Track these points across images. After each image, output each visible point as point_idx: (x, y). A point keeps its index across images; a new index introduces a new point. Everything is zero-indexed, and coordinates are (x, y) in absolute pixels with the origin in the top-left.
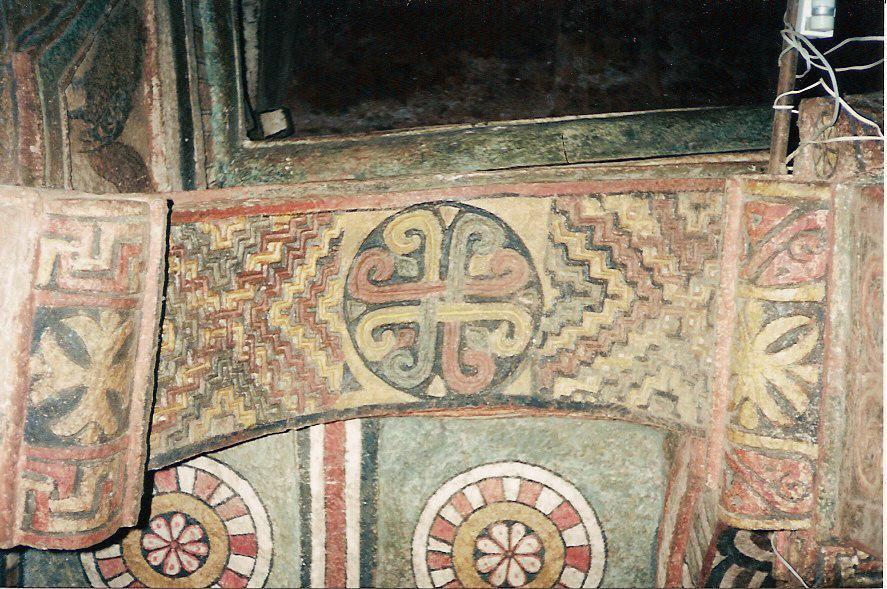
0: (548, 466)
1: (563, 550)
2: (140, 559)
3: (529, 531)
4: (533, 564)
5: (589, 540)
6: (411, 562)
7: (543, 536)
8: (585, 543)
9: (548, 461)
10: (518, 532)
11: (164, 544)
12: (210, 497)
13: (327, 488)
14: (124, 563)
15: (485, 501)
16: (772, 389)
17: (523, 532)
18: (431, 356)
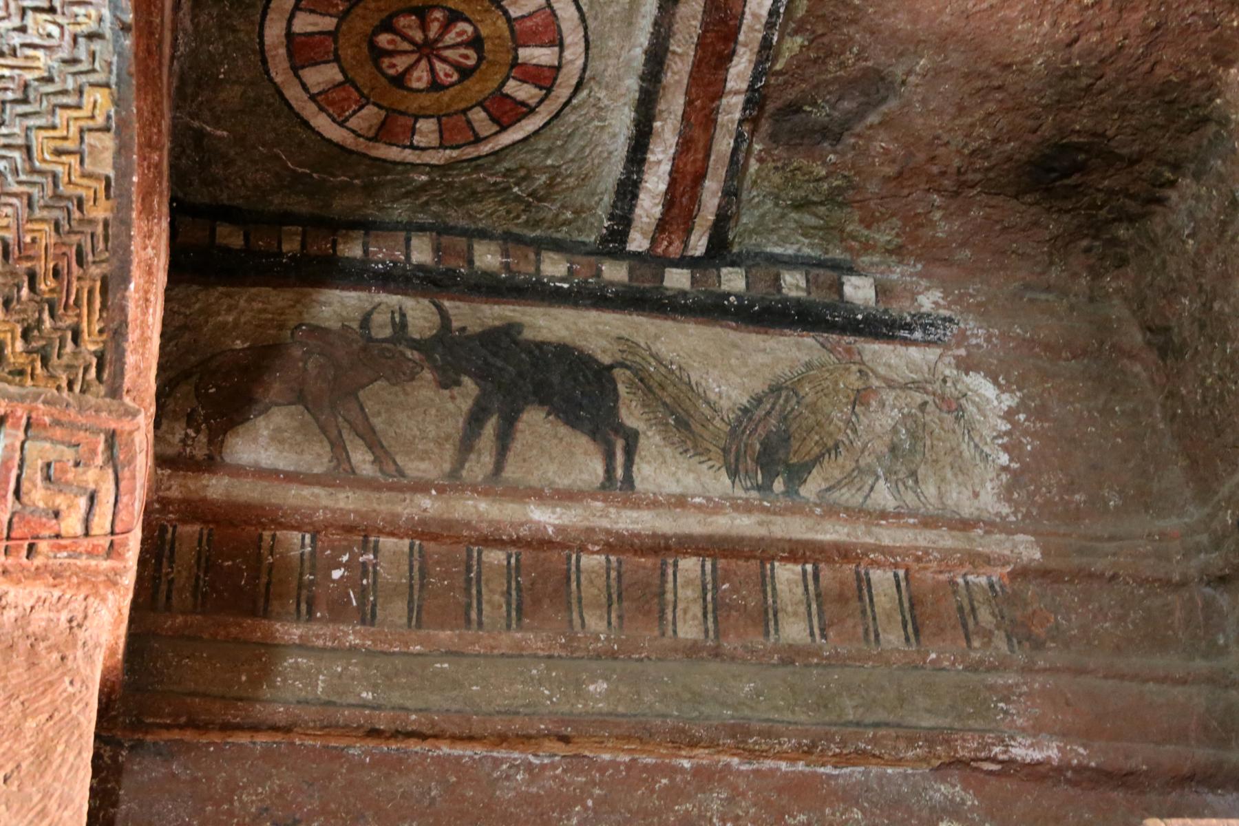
2: (446, 96)
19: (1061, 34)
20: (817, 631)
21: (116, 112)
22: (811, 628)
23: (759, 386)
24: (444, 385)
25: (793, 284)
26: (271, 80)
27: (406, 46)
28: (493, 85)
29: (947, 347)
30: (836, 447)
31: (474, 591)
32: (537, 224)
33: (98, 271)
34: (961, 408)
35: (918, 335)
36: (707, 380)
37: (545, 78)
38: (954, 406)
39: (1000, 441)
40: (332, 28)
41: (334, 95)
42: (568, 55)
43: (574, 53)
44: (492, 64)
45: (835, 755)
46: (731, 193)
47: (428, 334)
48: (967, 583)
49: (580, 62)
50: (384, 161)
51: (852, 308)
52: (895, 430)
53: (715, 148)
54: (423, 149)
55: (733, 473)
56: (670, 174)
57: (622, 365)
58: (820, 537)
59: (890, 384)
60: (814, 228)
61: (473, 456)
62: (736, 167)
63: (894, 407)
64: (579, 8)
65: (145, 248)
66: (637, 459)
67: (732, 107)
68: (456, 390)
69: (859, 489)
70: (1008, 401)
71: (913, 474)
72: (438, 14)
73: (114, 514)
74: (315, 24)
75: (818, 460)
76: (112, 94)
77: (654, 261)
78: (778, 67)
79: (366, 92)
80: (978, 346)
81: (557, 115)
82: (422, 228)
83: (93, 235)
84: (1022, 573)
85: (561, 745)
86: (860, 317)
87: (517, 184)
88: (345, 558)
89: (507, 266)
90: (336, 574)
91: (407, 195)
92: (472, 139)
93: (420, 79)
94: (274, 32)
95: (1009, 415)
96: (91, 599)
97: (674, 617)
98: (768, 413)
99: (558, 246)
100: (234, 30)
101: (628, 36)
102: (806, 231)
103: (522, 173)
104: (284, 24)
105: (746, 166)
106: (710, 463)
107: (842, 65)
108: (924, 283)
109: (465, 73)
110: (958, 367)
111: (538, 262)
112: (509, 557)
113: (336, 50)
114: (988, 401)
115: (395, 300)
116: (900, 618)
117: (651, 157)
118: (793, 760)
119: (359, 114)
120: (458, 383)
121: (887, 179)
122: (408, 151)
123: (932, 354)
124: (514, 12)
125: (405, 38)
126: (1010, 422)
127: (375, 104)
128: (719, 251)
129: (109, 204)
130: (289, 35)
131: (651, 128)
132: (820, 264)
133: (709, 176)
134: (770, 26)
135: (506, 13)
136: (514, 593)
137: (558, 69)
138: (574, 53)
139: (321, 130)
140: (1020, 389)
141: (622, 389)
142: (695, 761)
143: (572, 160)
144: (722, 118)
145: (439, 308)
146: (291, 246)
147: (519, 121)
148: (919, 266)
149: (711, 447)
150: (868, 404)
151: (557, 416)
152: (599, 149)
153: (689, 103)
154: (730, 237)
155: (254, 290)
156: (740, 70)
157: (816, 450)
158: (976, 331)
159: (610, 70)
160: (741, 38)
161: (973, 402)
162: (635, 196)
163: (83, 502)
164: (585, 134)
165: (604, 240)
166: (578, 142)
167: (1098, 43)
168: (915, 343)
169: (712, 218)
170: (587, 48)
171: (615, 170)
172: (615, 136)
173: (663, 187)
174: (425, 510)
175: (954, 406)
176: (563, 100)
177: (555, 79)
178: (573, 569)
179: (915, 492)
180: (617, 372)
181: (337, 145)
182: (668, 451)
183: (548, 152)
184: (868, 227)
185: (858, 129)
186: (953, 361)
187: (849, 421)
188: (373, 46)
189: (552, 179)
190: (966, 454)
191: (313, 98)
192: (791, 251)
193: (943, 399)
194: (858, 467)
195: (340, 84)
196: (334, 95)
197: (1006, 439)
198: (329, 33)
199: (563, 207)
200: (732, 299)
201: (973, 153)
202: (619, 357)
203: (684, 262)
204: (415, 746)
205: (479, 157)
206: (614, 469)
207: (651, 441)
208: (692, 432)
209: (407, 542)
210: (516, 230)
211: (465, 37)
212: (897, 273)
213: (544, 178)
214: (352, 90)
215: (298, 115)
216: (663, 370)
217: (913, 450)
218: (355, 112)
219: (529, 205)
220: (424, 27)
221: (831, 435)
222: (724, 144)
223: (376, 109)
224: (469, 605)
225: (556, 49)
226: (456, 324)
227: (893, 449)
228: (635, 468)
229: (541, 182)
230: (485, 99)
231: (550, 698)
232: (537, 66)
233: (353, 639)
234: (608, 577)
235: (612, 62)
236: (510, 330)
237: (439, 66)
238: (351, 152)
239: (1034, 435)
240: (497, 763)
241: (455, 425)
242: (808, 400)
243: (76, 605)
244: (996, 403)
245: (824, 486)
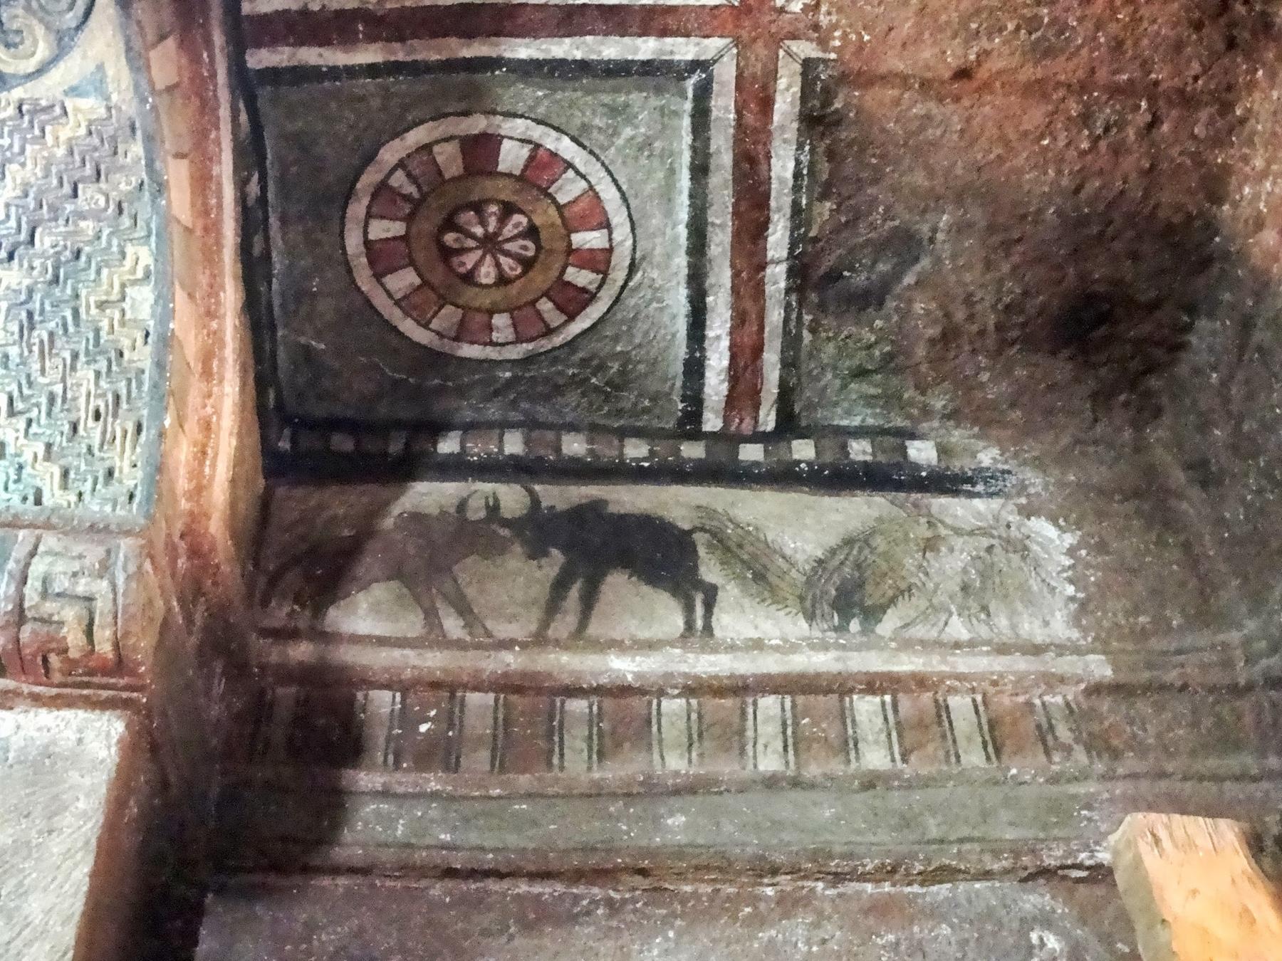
2: (514, 289)
12: (407, 198)
14: (519, 308)
19: (1065, 182)
20: (898, 757)
22: (892, 754)
23: (833, 540)
24: (532, 557)
25: (860, 450)
26: (358, 289)
28: (554, 273)
29: (1008, 497)
30: (909, 590)
31: (556, 739)
32: (619, 413)
34: (1026, 548)
35: (980, 488)
36: (782, 538)
37: (599, 261)
38: (1019, 547)
39: (1065, 575)
40: (402, 232)
41: (416, 299)
42: (617, 236)
43: (622, 233)
44: (551, 252)
45: (920, 873)
46: (789, 363)
47: (518, 514)
48: (1043, 704)
49: (629, 242)
51: (917, 467)
52: (965, 571)
53: (767, 321)
54: (503, 345)
55: (810, 617)
56: (731, 348)
57: (702, 529)
58: (895, 668)
59: (958, 532)
60: (873, 397)
61: (558, 616)
62: (791, 341)
63: (962, 551)
64: (619, 189)
65: (205, 406)
66: (716, 610)
67: (777, 277)
68: (544, 561)
69: (933, 625)
70: (1069, 539)
71: (985, 609)
72: (494, 208)
74: (388, 230)
75: (893, 601)
77: (729, 439)
78: (812, 234)
80: (1038, 495)
81: (617, 300)
82: (513, 426)
84: (1096, 690)
85: (638, 878)
86: (924, 474)
87: (595, 375)
88: (433, 713)
89: (591, 452)
90: (424, 728)
91: (496, 393)
93: (487, 274)
94: (353, 242)
95: (1071, 552)
97: (755, 752)
98: (842, 563)
99: (639, 433)
101: (669, 213)
102: (869, 400)
103: (595, 362)
105: (799, 337)
106: (788, 610)
107: (873, 227)
108: (981, 444)
109: (528, 264)
110: (1020, 513)
111: (623, 446)
112: (590, 707)
114: (1052, 541)
115: (487, 487)
116: (980, 739)
117: (710, 333)
118: (878, 881)
120: (546, 554)
121: (932, 342)
122: (489, 349)
123: (996, 503)
124: (562, 199)
126: (1072, 557)
127: (452, 304)
128: (789, 425)
130: (367, 243)
131: (705, 304)
132: (883, 432)
133: (766, 348)
134: (796, 188)
135: (554, 201)
136: (595, 737)
137: (610, 250)
138: (622, 233)
140: (1079, 529)
141: (702, 551)
142: (779, 888)
143: (640, 346)
144: (769, 289)
145: (531, 493)
146: (395, 447)
147: (584, 308)
148: (976, 429)
149: (788, 596)
150: (938, 551)
151: (639, 577)
152: (663, 332)
153: (736, 275)
154: (797, 410)
155: (362, 488)
156: (778, 239)
157: (890, 593)
158: (1035, 481)
159: (658, 251)
160: (773, 204)
161: (1038, 543)
162: (702, 375)
164: (647, 317)
165: (681, 423)
166: (642, 326)
167: (1101, 188)
168: (978, 495)
169: (776, 391)
170: (633, 229)
171: (681, 350)
172: (674, 317)
173: (726, 363)
174: (508, 665)
175: (1020, 547)
176: (621, 283)
177: (609, 262)
178: (654, 713)
179: (988, 624)
180: (700, 538)
181: (425, 347)
182: (746, 602)
183: (616, 339)
184: (923, 393)
185: (898, 289)
186: (1015, 509)
187: (920, 566)
189: (624, 365)
190: (1035, 588)
191: (397, 303)
192: (856, 421)
193: (1008, 541)
194: (932, 606)
195: (419, 287)
196: (416, 299)
197: (1070, 573)
198: (401, 238)
199: (640, 395)
200: (803, 465)
201: (1007, 307)
202: (697, 523)
203: (757, 437)
204: (493, 885)
205: (554, 349)
206: (694, 621)
207: (730, 593)
208: (770, 584)
209: (492, 696)
210: (602, 422)
212: (958, 436)
213: (615, 366)
216: (739, 531)
217: (983, 589)
218: (436, 313)
219: (608, 395)
220: (483, 223)
221: (903, 578)
222: (775, 316)
224: (551, 752)
225: (605, 231)
226: (544, 504)
227: (965, 588)
228: (714, 619)
229: (614, 370)
231: (628, 833)
232: (591, 250)
233: (434, 786)
234: (689, 718)
235: (658, 240)
236: (596, 507)
237: (503, 260)
239: (1096, 567)
240: (577, 899)
241: (541, 591)
242: (881, 549)
244: (1058, 542)
245: (899, 624)
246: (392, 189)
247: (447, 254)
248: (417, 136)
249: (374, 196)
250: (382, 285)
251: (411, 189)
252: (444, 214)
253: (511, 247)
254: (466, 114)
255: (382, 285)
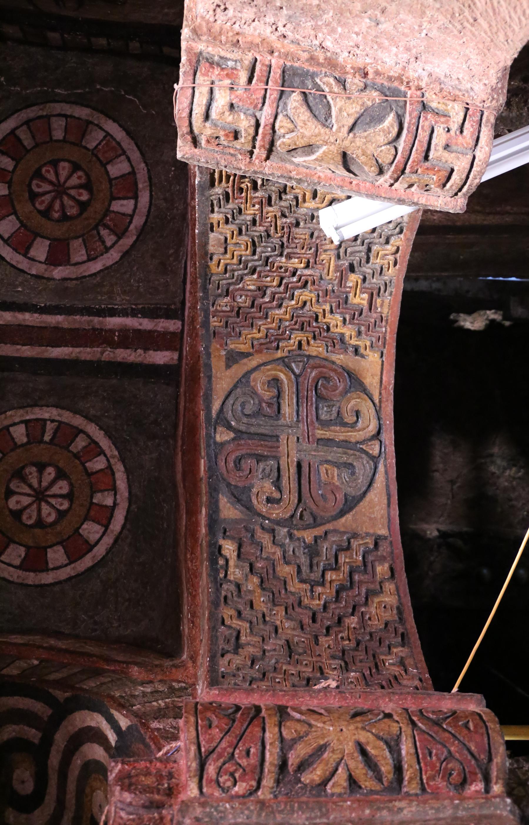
0: (125, 532)
1: (44, 545)
3: (61, 514)
4: (30, 517)
5: (53, 569)
6: (35, 405)
7: (58, 528)
8: (51, 566)
9: (129, 530)
10: (61, 504)
11: (62, 180)
12: (106, 227)
13: (112, 331)
15: (93, 473)
16: (321, 749)
17: (61, 508)
18: (252, 430)
21: (207, 262)
27: (73, 192)
33: (217, 190)
40: (114, 202)
41: (111, 154)
50: (82, 105)
54: (59, 115)
72: (56, 215)
73: (192, 103)
74: (122, 205)
76: (210, 271)
79: (94, 158)
83: (220, 207)
92: (31, 124)
94: (144, 199)
96: (212, 19)
100: (165, 199)
104: (139, 204)
109: (38, 174)
113: (111, 188)
119: (97, 142)
125: (73, 198)
129: (211, 221)
130: (136, 197)
135: (18, 218)
139: (120, 129)
146: (135, 45)
155: (153, 22)
163: (213, 115)
181: (110, 117)
188: (90, 190)
195: (108, 163)
196: (111, 154)
211: (40, 200)
214: (101, 159)
215: (132, 138)
218: (99, 144)
223: (88, 146)
230: (25, 155)
238: (102, 112)
243: (222, 18)
246: (116, 234)
247: (87, 186)
248: (96, 266)
249: (126, 230)
250: (132, 166)
251: (104, 232)
252: (85, 215)
253: (47, 187)
254: (65, 279)
255: (132, 166)
